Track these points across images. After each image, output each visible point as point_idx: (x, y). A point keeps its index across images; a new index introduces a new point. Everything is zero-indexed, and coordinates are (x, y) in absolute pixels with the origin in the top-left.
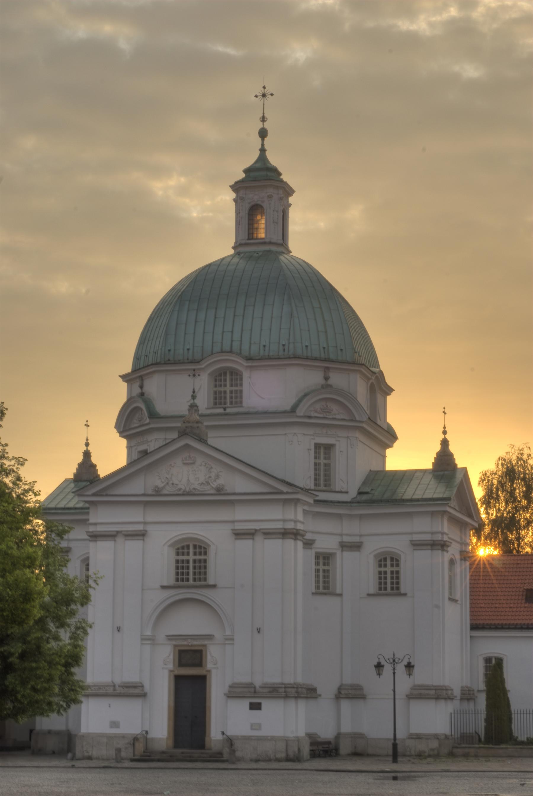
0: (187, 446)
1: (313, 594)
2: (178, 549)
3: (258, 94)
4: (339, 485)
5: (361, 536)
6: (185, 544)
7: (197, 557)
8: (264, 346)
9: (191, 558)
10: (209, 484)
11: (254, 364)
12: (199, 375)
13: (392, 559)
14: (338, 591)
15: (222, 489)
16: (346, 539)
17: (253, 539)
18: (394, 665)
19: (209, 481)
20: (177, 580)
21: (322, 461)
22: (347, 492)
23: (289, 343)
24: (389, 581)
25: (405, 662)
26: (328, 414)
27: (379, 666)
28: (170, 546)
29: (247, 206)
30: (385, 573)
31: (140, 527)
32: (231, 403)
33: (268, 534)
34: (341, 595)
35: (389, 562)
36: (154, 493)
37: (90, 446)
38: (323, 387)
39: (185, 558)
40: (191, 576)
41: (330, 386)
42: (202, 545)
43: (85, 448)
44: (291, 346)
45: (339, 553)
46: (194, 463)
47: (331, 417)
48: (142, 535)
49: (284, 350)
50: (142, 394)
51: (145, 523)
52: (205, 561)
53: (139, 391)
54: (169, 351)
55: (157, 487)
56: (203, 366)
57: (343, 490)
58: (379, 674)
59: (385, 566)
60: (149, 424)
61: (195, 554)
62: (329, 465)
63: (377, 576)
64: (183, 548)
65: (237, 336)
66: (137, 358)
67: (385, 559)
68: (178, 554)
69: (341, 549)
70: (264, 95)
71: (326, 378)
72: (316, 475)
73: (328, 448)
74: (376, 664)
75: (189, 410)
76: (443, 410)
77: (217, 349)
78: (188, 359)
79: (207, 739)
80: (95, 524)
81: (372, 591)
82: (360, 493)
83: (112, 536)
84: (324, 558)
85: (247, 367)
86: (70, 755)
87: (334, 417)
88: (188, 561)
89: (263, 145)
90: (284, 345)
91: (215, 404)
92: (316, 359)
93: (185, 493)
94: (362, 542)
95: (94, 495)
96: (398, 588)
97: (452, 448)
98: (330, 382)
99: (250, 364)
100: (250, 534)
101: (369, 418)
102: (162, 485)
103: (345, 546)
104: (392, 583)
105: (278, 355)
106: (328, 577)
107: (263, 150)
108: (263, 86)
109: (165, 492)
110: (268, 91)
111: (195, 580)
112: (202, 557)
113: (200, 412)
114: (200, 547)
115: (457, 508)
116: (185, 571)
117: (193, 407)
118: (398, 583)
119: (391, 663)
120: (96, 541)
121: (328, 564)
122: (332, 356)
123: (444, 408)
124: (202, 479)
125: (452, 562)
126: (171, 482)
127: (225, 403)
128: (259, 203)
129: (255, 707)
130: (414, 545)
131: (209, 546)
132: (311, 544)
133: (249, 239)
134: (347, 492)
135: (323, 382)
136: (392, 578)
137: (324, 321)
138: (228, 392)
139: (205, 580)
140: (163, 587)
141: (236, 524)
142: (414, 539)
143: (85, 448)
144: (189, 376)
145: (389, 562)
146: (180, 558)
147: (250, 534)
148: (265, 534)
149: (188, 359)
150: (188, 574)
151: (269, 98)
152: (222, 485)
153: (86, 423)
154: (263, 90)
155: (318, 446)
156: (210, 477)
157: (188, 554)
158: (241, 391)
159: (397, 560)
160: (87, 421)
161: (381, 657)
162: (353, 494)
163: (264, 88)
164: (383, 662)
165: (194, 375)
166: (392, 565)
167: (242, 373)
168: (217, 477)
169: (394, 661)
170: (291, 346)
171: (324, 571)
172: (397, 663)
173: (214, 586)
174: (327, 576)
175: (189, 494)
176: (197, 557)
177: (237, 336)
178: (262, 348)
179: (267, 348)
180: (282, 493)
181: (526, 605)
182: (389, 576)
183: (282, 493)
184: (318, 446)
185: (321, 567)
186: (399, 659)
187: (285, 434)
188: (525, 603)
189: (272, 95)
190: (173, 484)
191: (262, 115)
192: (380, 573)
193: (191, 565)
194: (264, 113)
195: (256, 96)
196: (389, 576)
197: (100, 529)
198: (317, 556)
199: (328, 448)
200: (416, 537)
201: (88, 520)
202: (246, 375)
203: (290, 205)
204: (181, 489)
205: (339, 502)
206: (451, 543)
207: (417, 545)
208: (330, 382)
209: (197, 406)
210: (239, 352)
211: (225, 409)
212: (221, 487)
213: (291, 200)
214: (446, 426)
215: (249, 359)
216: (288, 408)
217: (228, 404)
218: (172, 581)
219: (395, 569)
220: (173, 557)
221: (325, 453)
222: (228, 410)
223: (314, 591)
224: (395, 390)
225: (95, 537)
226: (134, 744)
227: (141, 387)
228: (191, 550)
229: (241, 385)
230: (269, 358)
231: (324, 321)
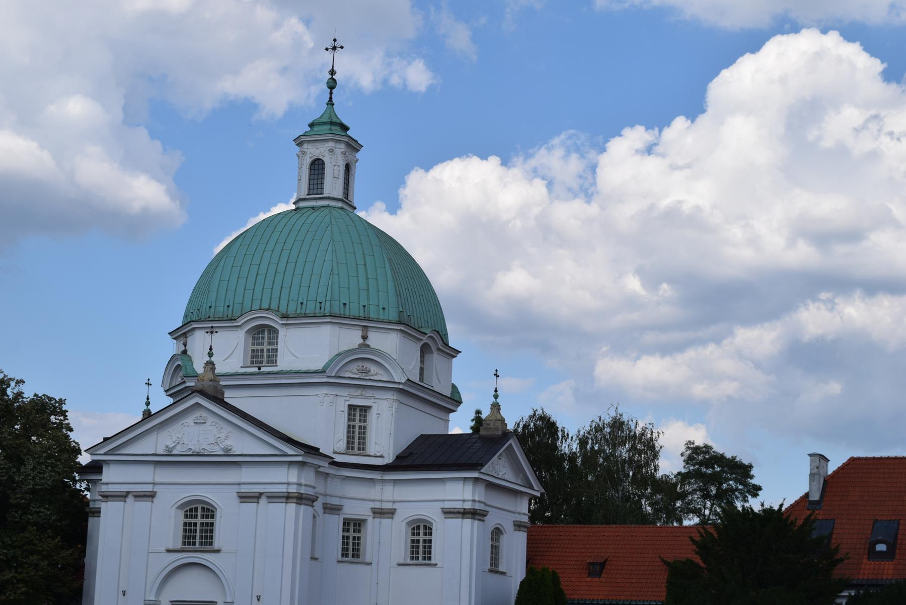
0: (197, 405)
1: (338, 561)
2: (187, 511)
3: (329, 47)
4: (372, 448)
5: (394, 502)
6: (194, 506)
7: (205, 520)
8: (302, 303)
10: (219, 445)
11: (289, 322)
12: (216, 332)
13: (425, 527)
15: (230, 450)
16: (377, 505)
17: (258, 503)
19: (218, 442)
20: (184, 543)
21: (357, 424)
22: (382, 457)
23: (326, 301)
24: (421, 550)
26: (364, 375)
28: (180, 507)
29: (308, 161)
30: (418, 541)
31: (149, 488)
32: (268, 362)
33: (273, 497)
35: (422, 531)
36: (165, 453)
37: (150, 405)
38: (360, 346)
39: (193, 521)
40: (198, 540)
41: (369, 346)
42: (211, 508)
43: (145, 407)
44: (328, 304)
45: (370, 520)
46: (205, 423)
47: (368, 378)
48: (151, 496)
49: (321, 308)
50: (185, 352)
51: (154, 484)
52: (212, 524)
53: (183, 348)
54: (210, 307)
55: (167, 446)
56: (239, 324)
57: (378, 454)
59: (418, 534)
60: (184, 382)
61: (203, 517)
62: (365, 428)
63: (409, 544)
64: (191, 510)
65: (276, 294)
66: (186, 316)
67: (418, 527)
68: (186, 516)
70: (334, 48)
71: (365, 338)
72: (348, 437)
73: (365, 409)
75: (204, 368)
76: (495, 372)
77: (256, 306)
78: (227, 316)
80: (107, 484)
81: (402, 561)
82: (398, 457)
83: (123, 496)
84: (355, 525)
85: (282, 324)
87: (372, 378)
88: (195, 524)
89: (331, 98)
90: (320, 303)
91: (252, 362)
92: (354, 318)
93: (195, 453)
94: (395, 509)
95: (105, 454)
96: (430, 558)
97: (504, 413)
98: (368, 342)
99: (285, 322)
100: (256, 497)
101: (408, 379)
102: (174, 445)
103: (379, 513)
104: (424, 553)
105: (314, 313)
106: (358, 544)
107: (330, 102)
108: (334, 38)
109: (175, 452)
110: (338, 44)
111: (201, 544)
112: (209, 521)
113: (217, 371)
114: (208, 510)
115: (510, 476)
117: (210, 365)
118: (430, 553)
120: (107, 501)
121: (359, 531)
122: (372, 315)
123: (497, 371)
124: (212, 440)
125: (497, 532)
126: (183, 442)
127: (262, 362)
128: (320, 157)
131: (216, 509)
133: (308, 195)
134: (382, 457)
135: (361, 341)
136: (425, 547)
137: (367, 278)
138: (265, 351)
139: (211, 544)
140: (169, 551)
141: (242, 486)
142: (446, 507)
143: (145, 407)
144: (207, 332)
145: (422, 531)
146: (188, 520)
147: (256, 497)
148: (268, 497)
149: (227, 316)
150: (195, 537)
152: (231, 446)
153: (147, 382)
155: (351, 407)
156: (219, 437)
157: (196, 517)
158: (277, 349)
159: (431, 529)
160: (149, 380)
162: (389, 459)
163: (335, 40)
165: (212, 332)
166: (425, 534)
167: (278, 331)
168: (227, 438)
170: (328, 304)
171: (354, 538)
173: (218, 551)
174: (202, 539)
175: (198, 455)
176: (205, 520)
177: (276, 294)
178: (299, 305)
179: (304, 306)
180: (286, 455)
181: (588, 579)
182: (421, 544)
183: (286, 455)
184: (351, 407)
185: (351, 534)
187: (317, 395)
188: (588, 577)
189: (342, 47)
190: (183, 444)
191: (331, 68)
192: (413, 541)
193: (198, 528)
194: (333, 66)
195: (327, 49)
196: (421, 544)
197: (111, 488)
198: (346, 523)
199: (365, 409)
200: (448, 505)
201: (101, 480)
202: (282, 332)
203: (357, 161)
204: (191, 449)
206: (488, 512)
207: (449, 513)
208: (368, 342)
209: (214, 365)
210: (277, 309)
211: (259, 369)
212: (229, 448)
213: (358, 155)
214: (497, 389)
215: (284, 317)
216: (319, 366)
217: (264, 364)
218: (179, 545)
219: (427, 538)
220: (181, 519)
221: (360, 416)
222: (263, 369)
223: (340, 558)
224: (460, 352)
225: (106, 497)
227: (185, 345)
228: (199, 513)
229: (277, 344)
230: (306, 316)
231: (367, 278)
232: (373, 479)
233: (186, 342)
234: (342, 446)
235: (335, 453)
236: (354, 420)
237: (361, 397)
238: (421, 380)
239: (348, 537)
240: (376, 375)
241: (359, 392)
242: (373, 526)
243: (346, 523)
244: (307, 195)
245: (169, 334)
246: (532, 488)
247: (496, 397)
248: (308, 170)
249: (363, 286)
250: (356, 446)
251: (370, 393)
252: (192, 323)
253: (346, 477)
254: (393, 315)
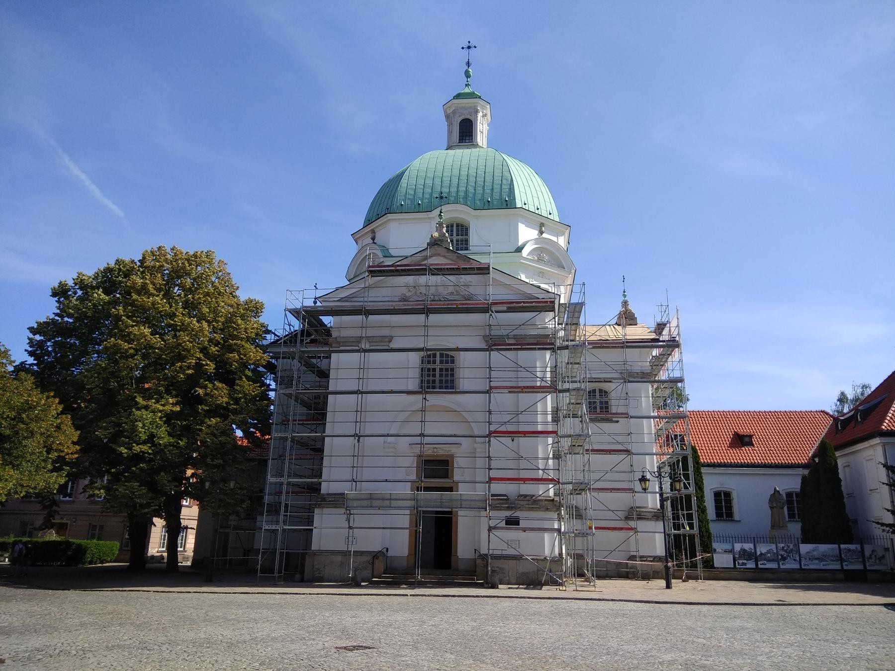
9: (438, 366)
18: (660, 479)
35: (597, 394)
49: (507, 205)
52: (452, 370)
61: (441, 362)
64: (429, 356)
70: (469, 47)
74: (641, 477)
79: (453, 558)
86: (298, 576)
88: (434, 370)
112: (449, 366)
116: (431, 378)
119: (657, 477)
129: (512, 522)
133: (459, 143)
145: (597, 394)
151: (473, 49)
154: (468, 44)
160: (316, 284)
163: (469, 42)
164: (648, 476)
169: (660, 475)
172: (663, 477)
176: (444, 366)
186: (666, 473)
195: (463, 48)
226: (373, 563)
227: (373, 239)
233: (375, 236)
244: (459, 143)
245: (352, 235)
247: (625, 296)
248: (458, 125)
249: (535, 194)
252: (388, 215)
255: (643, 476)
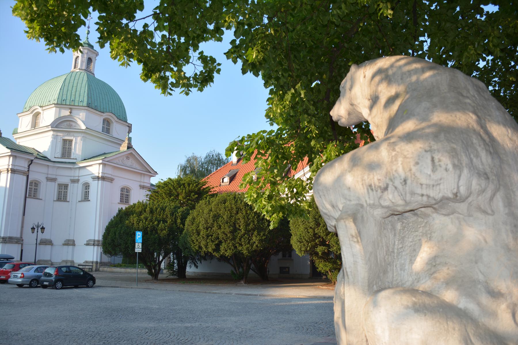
14: (68, 200)
16: (72, 178)
25: (41, 227)
27: (33, 229)
34: (69, 202)
58: (33, 232)
69: (70, 182)
73: (71, 141)
98: (71, 114)
130: (93, 179)
132: (55, 180)
134: (76, 159)
161: (34, 224)
162: (80, 160)
164: (35, 227)
169: (38, 226)
205: (69, 163)
221: (69, 144)
232: (70, 168)
234: (59, 155)
235: (55, 158)
236: (66, 146)
237: (68, 135)
238: (102, 131)
239: (61, 192)
240: (75, 127)
241: (67, 133)
242: (70, 186)
243: (60, 185)
246: (150, 173)
250: (66, 155)
251: (72, 134)
253: (59, 167)
254: (85, 104)
255: (33, 227)
